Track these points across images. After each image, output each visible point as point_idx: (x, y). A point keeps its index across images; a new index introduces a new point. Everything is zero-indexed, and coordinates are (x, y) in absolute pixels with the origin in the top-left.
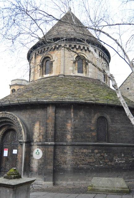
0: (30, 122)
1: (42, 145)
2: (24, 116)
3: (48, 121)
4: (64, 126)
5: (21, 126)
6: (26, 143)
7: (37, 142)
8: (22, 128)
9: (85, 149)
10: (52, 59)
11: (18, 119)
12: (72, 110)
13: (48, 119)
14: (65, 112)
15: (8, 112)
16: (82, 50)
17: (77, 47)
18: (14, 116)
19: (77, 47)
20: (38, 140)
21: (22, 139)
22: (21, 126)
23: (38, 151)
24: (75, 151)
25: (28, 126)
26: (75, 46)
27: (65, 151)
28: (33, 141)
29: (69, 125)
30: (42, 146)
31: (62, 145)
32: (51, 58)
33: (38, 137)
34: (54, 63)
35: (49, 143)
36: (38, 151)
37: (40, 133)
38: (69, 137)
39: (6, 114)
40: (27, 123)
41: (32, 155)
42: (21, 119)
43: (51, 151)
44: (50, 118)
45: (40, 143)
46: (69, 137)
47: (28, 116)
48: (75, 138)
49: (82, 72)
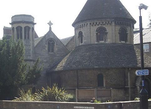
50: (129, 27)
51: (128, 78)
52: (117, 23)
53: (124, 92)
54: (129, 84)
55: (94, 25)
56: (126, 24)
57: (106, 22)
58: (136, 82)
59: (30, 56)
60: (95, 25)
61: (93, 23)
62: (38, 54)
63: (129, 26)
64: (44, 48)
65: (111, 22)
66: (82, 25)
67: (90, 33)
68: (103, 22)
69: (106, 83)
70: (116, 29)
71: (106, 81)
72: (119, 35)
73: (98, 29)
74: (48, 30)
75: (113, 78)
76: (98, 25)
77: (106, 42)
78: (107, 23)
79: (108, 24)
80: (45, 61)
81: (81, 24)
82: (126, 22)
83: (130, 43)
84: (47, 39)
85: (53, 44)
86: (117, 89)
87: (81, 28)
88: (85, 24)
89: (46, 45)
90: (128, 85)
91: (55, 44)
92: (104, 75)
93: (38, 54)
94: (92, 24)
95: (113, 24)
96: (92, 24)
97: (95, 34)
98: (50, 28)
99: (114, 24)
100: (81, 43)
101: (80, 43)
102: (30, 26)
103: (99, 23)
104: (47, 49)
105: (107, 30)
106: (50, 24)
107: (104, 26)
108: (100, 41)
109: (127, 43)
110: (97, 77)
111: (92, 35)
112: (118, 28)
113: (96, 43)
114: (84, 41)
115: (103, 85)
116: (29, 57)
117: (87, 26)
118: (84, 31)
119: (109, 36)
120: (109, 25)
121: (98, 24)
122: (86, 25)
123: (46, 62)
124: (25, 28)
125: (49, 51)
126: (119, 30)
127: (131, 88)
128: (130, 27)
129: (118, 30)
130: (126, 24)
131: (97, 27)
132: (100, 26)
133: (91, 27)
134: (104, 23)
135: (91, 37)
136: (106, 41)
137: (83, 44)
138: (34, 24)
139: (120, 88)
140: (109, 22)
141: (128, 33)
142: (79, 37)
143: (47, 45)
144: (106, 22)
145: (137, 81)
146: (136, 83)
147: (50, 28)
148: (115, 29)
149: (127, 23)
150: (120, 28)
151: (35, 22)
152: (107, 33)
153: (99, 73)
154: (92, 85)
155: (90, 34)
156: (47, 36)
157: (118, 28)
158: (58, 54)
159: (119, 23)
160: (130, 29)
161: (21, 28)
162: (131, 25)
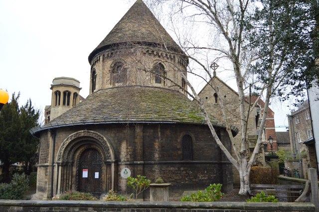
0: (116, 141)
1: (129, 165)
2: (109, 135)
3: (136, 141)
4: (151, 146)
5: (109, 145)
6: (114, 162)
7: (125, 161)
8: (110, 148)
9: (171, 167)
11: (105, 139)
12: (159, 129)
13: (136, 138)
14: (152, 131)
15: (91, 131)
16: (159, 56)
17: (155, 53)
18: (100, 136)
19: (155, 53)
20: (125, 160)
21: (110, 159)
22: (109, 145)
23: (126, 170)
24: (163, 169)
25: (115, 146)
26: (153, 52)
27: (153, 169)
28: (120, 161)
29: (157, 144)
30: (131, 165)
31: (151, 164)
33: (126, 156)
35: (139, 162)
36: (126, 170)
37: (127, 152)
38: (157, 155)
40: (112, 142)
41: (120, 175)
42: (107, 139)
43: (140, 170)
44: (138, 137)
45: (128, 163)
46: (157, 155)
47: (113, 135)
48: (162, 156)
49: (160, 83)
112: (109, 63)
157: (109, 63)
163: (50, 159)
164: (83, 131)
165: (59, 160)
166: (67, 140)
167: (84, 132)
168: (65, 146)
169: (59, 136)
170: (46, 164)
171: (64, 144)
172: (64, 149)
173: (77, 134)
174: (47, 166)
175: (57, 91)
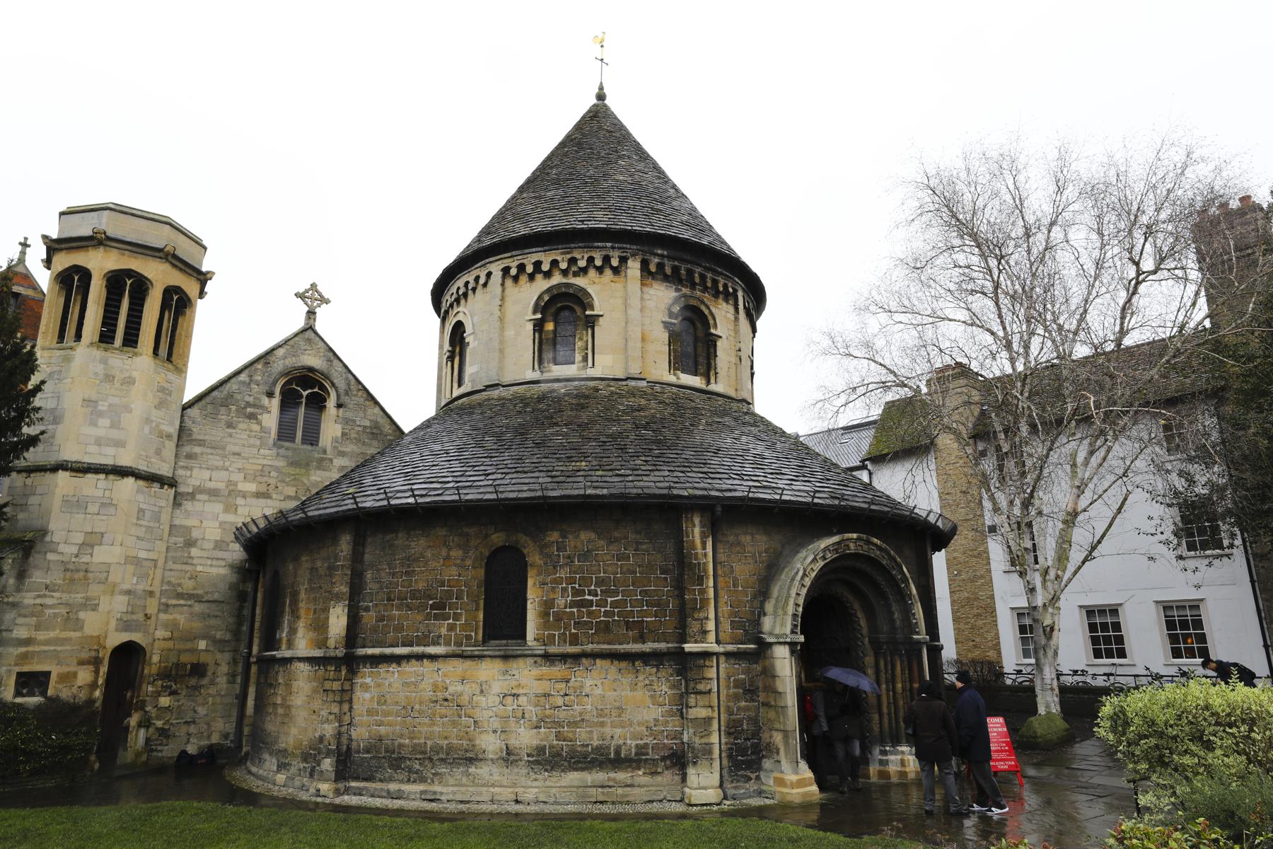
10: (715, 326)
15: (875, 540)
21: (918, 633)
32: (711, 322)
34: (719, 344)
39: (868, 542)
50: (724, 304)
51: (700, 580)
52: (653, 268)
53: (673, 687)
54: (711, 626)
55: (524, 279)
56: (709, 284)
57: (591, 260)
58: (763, 613)
59: (120, 444)
60: (532, 277)
61: (521, 268)
62: (201, 443)
63: (727, 301)
64: (252, 417)
65: (623, 260)
66: (467, 283)
67: (501, 319)
68: (573, 261)
69: (544, 614)
70: (650, 304)
71: (547, 605)
72: (666, 336)
73: (546, 298)
74: (300, 323)
75: (600, 582)
76: (548, 275)
77: (591, 372)
78: (598, 263)
79: (600, 270)
80: (251, 487)
81: (460, 283)
82: (709, 275)
83: (733, 394)
84: (279, 365)
85: (317, 403)
86: (624, 664)
87: (463, 301)
88: (477, 279)
89: (265, 400)
90: (705, 632)
91: (331, 403)
92: (534, 558)
93: (201, 443)
94: (514, 272)
95: (634, 267)
96: (514, 272)
97: (530, 326)
98: (311, 314)
99: (638, 273)
100: (460, 386)
101: (455, 385)
102: (159, 275)
103: (555, 263)
104: (271, 419)
105: (596, 303)
106: (312, 298)
107: (580, 281)
108: (554, 368)
109: (713, 387)
110: (481, 572)
111: (510, 333)
112: (663, 297)
113: (531, 375)
114: (469, 370)
115: (522, 635)
116: (110, 451)
117: (485, 285)
118: (471, 313)
119: (604, 332)
120: (608, 272)
121: (545, 267)
122: (482, 281)
123: (258, 495)
124: (116, 281)
125: (285, 433)
126: (669, 310)
127: (728, 655)
128: (731, 309)
129: (663, 306)
130: (709, 284)
131: (541, 285)
132: (557, 279)
133: (508, 291)
134: (582, 263)
135: (502, 342)
136: (585, 367)
137: (463, 390)
138: (203, 278)
139: (645, 658)
140: (607, 259)
141: (721, 337)
142: (451, 358)
143: (275, 403)
144: (591, 260)
145: (769, 607)
146: (767, 623)
147: (311, 314)
148: (642, 299)
149: (715, 282)
150: (676, 300)
151: (204, 269)
152: (591, 322)
153: (498, 539)
154: (444, 631)
155: (502, 329)
156: (281, 352)
158: (342, 454)
159: (668, 271)
160: (732, 318)
161: (85, 275)
162: (735, 291)
163: (711, 626)
164: (855, 536)
165: (793, 632)
166: (814, 560)
167: (859, 539)
168: (808, 582)
169: (731, 538)
170: (688, 647)
171: (805, 575)
172: (804, 591)
173: (838, 543)
174: (706, 655)
175: (129, 273)
